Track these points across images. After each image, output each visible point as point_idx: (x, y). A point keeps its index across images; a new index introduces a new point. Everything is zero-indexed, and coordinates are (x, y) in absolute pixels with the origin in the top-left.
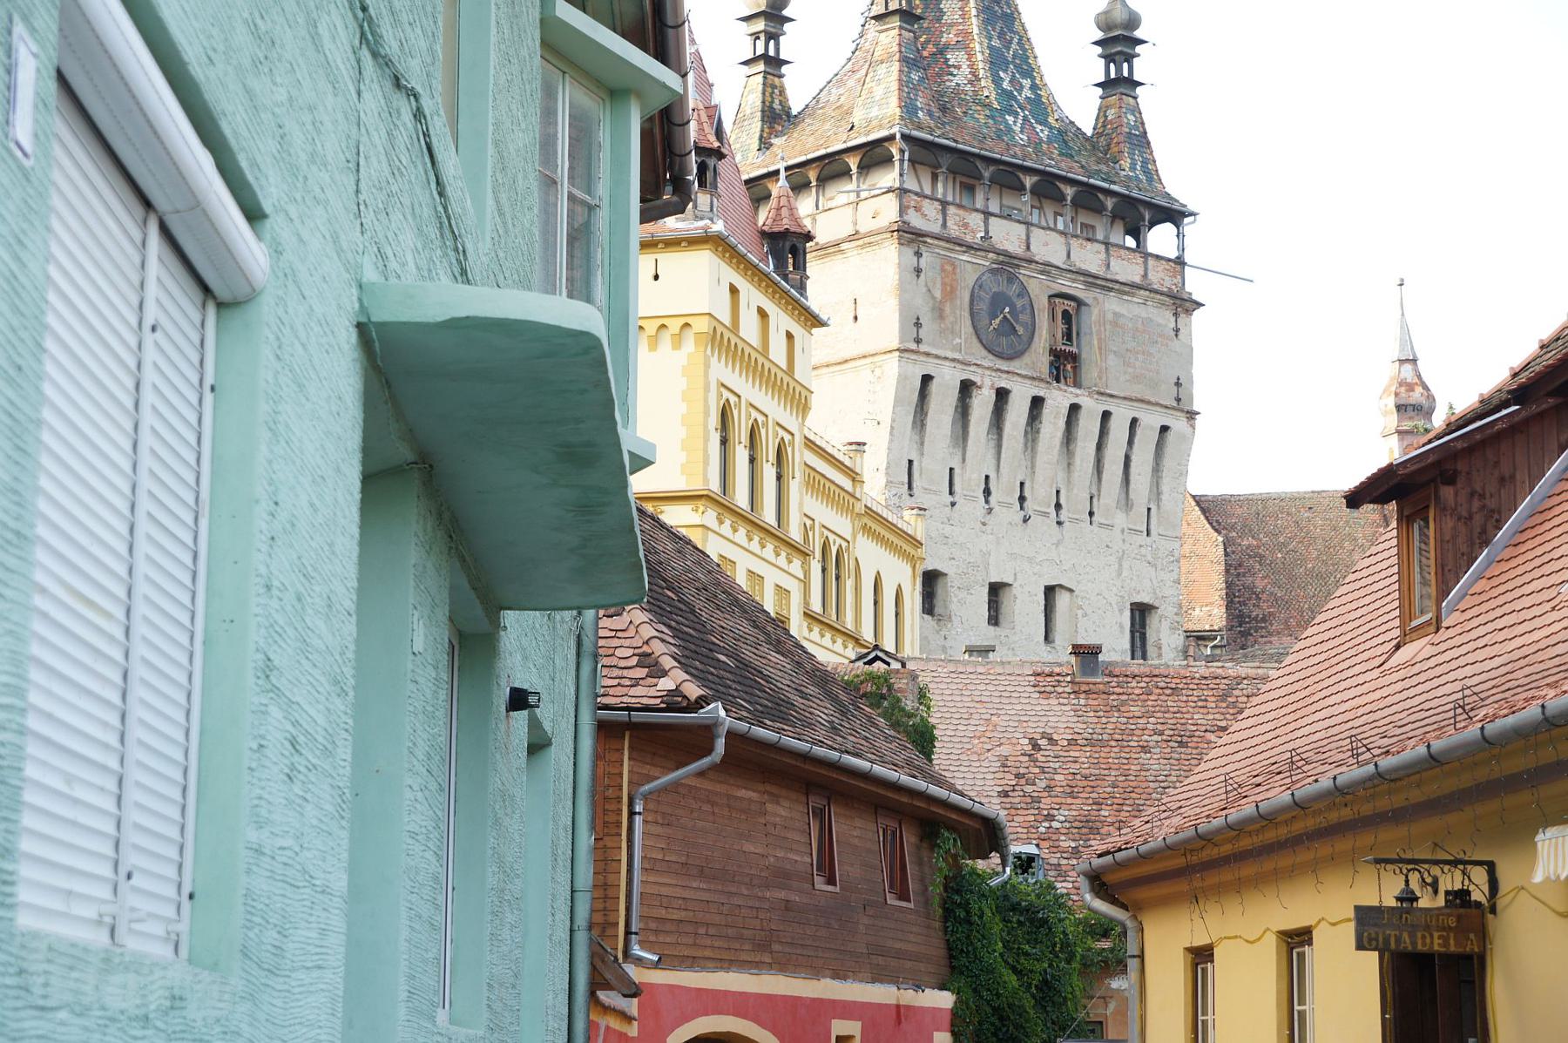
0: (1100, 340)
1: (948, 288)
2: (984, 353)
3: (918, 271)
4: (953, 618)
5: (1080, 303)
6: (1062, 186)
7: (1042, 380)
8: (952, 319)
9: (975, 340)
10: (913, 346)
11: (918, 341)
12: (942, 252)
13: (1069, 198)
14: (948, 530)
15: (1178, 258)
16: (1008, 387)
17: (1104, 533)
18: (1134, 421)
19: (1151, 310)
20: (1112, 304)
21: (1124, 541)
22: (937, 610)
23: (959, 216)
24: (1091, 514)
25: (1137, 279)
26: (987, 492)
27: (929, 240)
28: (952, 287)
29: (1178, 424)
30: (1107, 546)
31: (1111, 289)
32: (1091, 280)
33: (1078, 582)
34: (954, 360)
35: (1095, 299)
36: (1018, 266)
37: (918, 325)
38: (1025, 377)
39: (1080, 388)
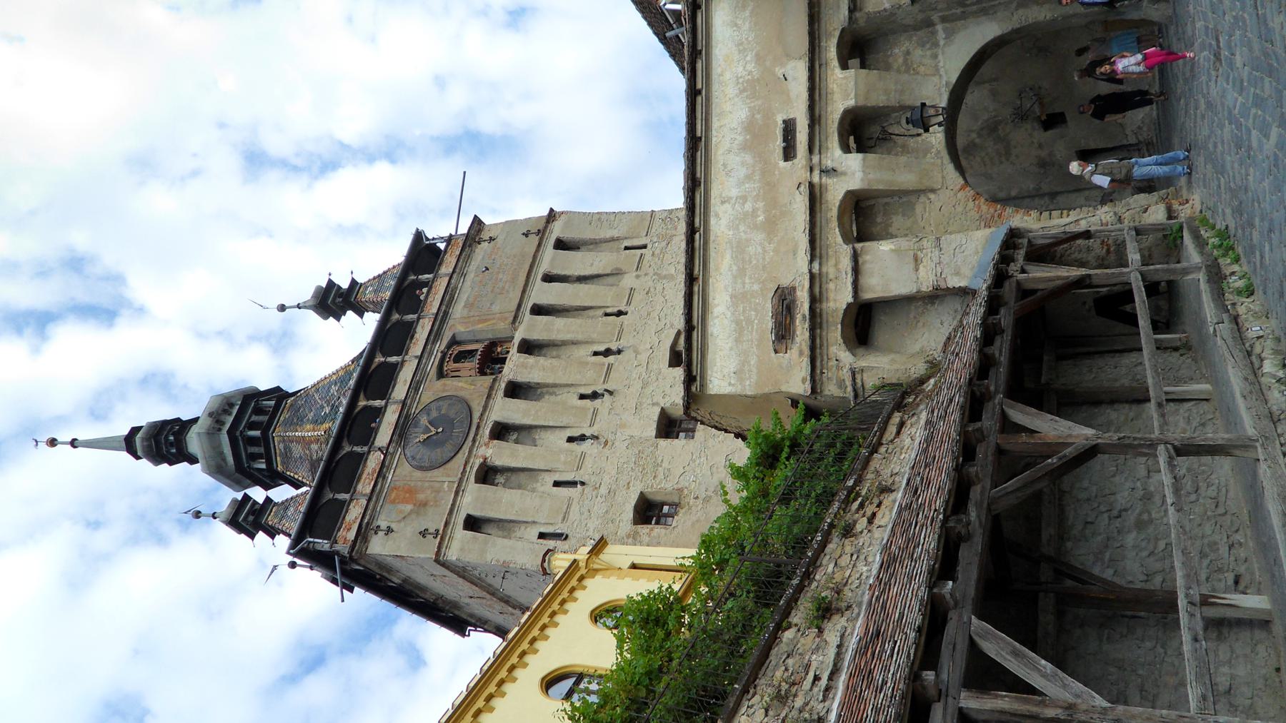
0: (481, 321)
1: (408, 495)
2: (460, 455)
5: (454, 342)
6: (373, 366)
7: (491, 388)
9: (448, 466)
10: (439, 536)
12: (380, 504)
14: (603, 490)
15: (445, 241)
16: (490, 426)
19: (471, 267)
20: (458, 311)
21: (646, 274)
22: (676, 501)
24: (620, 313)
26: (582, 438)
27: (366, 521)
28: (407, 492)
29: (557, 230)
31: (446, 313)
32: (434, 335)
33: (672, 326)
34: (457, 493)
36: (407, 416)
37: (424, 534)
38: (485, 408)
39: (513, 338)
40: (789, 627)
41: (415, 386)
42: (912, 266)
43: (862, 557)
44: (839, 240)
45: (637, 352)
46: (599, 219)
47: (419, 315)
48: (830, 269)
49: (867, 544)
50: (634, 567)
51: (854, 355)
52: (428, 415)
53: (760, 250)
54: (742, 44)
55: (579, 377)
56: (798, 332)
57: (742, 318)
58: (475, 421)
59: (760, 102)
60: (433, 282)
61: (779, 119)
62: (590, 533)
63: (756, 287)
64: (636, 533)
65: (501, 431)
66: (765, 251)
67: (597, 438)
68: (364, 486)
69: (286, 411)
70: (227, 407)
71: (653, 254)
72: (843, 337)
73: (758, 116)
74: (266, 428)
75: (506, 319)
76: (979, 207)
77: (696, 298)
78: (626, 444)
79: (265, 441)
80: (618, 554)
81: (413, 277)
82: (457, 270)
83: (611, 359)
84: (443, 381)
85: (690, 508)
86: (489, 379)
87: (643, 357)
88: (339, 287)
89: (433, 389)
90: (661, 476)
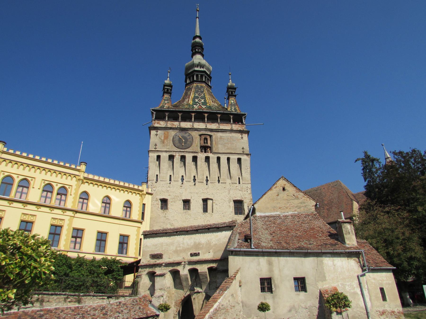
1: (166, 137)
3: (157, 135)
4: (169, 209)
7: (195, 152)
8: (167, 143)
10: (155, 150)
11: (155, 148)
13: (206, 116)
14: (168, 189)
17: (223, 185)
18: (228, 159)
20: (220, 134)
21: (230, 186)
23: (171, 123)
24: (219, 181)
25: (229, 129)
26: (183, 180)
29: (244, 158)
30: (224, 188)
31: (219, 131)
32: (212, 130)
35: (214, 134)
36: (188, 130)
37: (156, 145)
40: (38, 295)
41: (197, 130)
42: (160, 288)
43: (58, 303)
44: (170, 270)
45: (207, 189)
46: (248, 168)
47: (219, 123)
48: (163, 268)
49: (62, 303)
50: (144, 205)
51: (146, 274)
52: (188, 136)
53: (171, 249)
54: (220, 240)
55: (200, 175)
56: (153, 260)
57: (158, 246)
58: (185, 150)
59: (205, 246)
60: (230, 124)
61: (200, 252)
62: (158, 188)
63: (164, 249)
64: (157, 200)
65: (183, 158)
66: (171, 250)
67: (182, 184)
68: (170, 124)
69: (201, 85)
70: (202, 66)
71: (236, 187)
72: (150, 272)
73: (201, 246)
74: (197, 81)
75: (216, 150)
76: (179, 300)
77: (162, 234)
78: (181, 192)
79: (193, 81)
80: (148, 200)
81: (232, 116)
82: (232, 131)
83: (205, 182)
84: (199, 136)
85: (163, 213)
86: (199, 150)
87: (205, 191)
88: (235, 92)
89: (195, 134)
90: (172, 203)
